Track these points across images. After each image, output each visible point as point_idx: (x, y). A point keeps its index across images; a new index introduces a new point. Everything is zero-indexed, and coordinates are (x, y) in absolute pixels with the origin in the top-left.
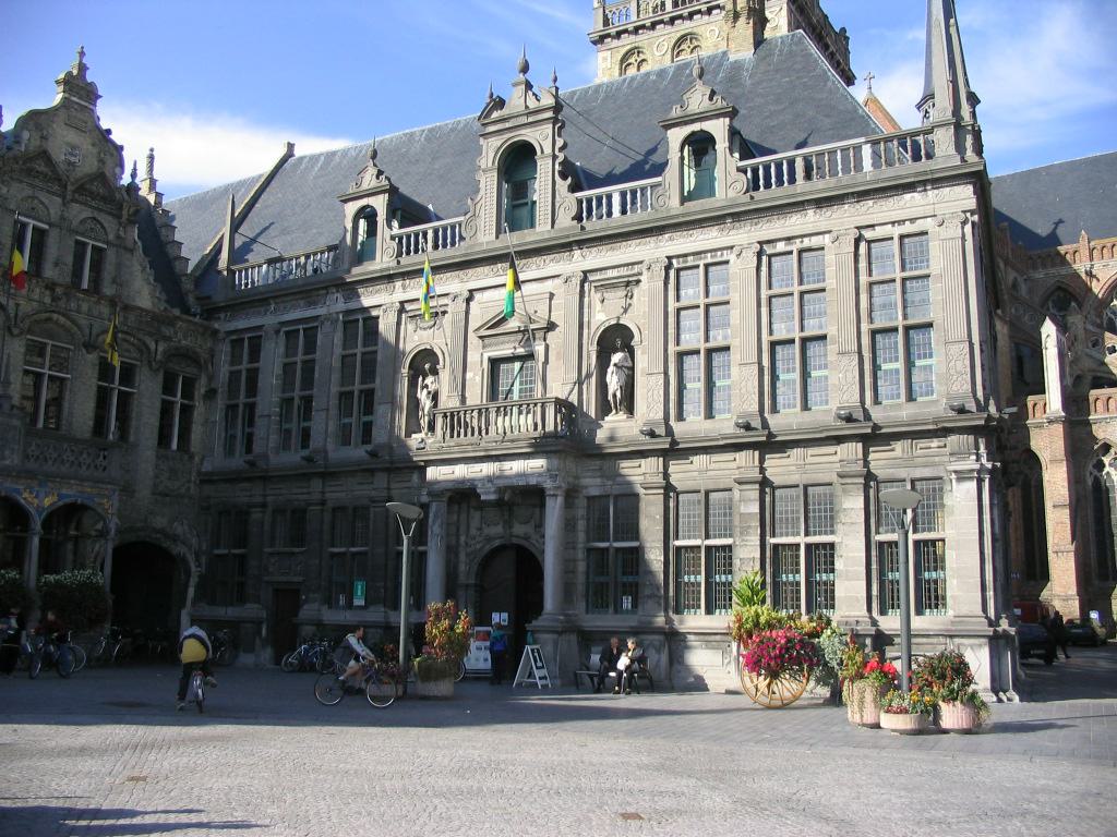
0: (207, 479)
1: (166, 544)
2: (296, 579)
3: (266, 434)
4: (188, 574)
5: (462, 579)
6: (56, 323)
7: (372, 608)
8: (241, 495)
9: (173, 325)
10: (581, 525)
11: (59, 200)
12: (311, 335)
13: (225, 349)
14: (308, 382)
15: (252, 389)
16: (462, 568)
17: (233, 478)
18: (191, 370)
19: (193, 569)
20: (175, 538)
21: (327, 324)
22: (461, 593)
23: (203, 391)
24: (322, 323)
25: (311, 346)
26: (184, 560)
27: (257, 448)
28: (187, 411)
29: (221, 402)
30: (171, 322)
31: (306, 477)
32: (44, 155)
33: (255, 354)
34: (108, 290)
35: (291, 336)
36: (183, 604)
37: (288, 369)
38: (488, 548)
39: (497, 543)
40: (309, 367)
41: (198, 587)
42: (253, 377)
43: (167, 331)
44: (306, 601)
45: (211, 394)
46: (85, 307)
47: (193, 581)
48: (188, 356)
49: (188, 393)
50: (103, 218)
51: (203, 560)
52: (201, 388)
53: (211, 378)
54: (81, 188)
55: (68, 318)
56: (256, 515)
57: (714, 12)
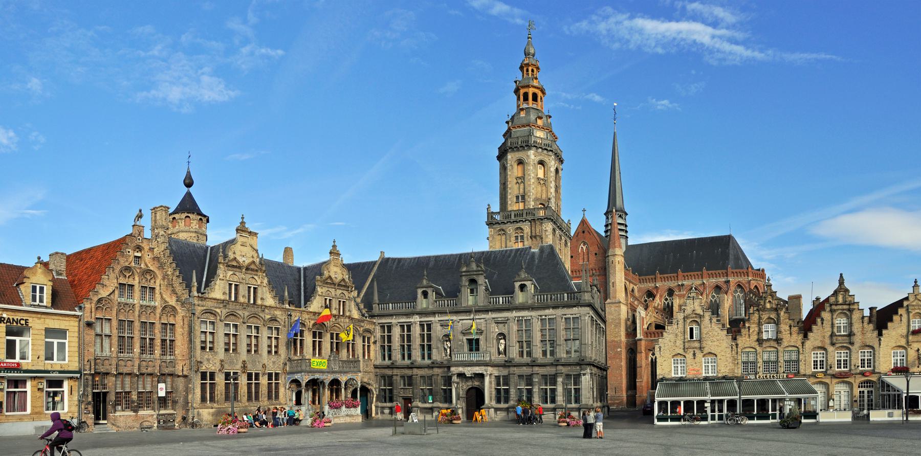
0: (376, 367)
1: (367, 386)
2: (410, 395)
3: (397, 356)
4: (373, 394)
5: (461, 396)
6: (336, 326)
7: (435, 403)
8: (388, 372)
9: (363, 322)
10: (493, 383)
11: (334, 290)
12: (409, 327)
13: (378, 328)
14: (409, 340)
15: (390, 341)
16: (461, 393)
17: (388, 367)
18: (369, 335)
19: (375, 393)
20: (369, 384)
21: (414, 324)
22: (461, 399)
23: (373, 341)
24: (412, 324)
25: (409, 330)
26: (372, 390)
27: (393, 358)
28: (369, 346)
29: (378, 344)
30: (363, 321)
31: (412, 368)
32: (330, 277)
33: (389, 330)
34: (348, 314)
35: (402, 327)
36: (372, 403)
37: (402, 336)
38: (468, 388)
39: (471, 387)
40: (409, 336)
41: (377, 397)
42: (389, 337)
43: (362, 324)
44: (413, 401)
45: (375, 342)
46: (342, 321)
47: (375, 396)
48: (368, 331)
49: (369, 342)
50: (344, 292)
51: (377, 390)
52: (372, 340)
53: (374, 337)
54: (339, 285)
55: (339, 324)
56: (395, 378)
57: (527, 221)
